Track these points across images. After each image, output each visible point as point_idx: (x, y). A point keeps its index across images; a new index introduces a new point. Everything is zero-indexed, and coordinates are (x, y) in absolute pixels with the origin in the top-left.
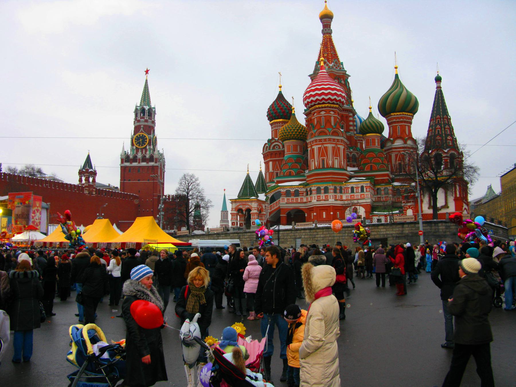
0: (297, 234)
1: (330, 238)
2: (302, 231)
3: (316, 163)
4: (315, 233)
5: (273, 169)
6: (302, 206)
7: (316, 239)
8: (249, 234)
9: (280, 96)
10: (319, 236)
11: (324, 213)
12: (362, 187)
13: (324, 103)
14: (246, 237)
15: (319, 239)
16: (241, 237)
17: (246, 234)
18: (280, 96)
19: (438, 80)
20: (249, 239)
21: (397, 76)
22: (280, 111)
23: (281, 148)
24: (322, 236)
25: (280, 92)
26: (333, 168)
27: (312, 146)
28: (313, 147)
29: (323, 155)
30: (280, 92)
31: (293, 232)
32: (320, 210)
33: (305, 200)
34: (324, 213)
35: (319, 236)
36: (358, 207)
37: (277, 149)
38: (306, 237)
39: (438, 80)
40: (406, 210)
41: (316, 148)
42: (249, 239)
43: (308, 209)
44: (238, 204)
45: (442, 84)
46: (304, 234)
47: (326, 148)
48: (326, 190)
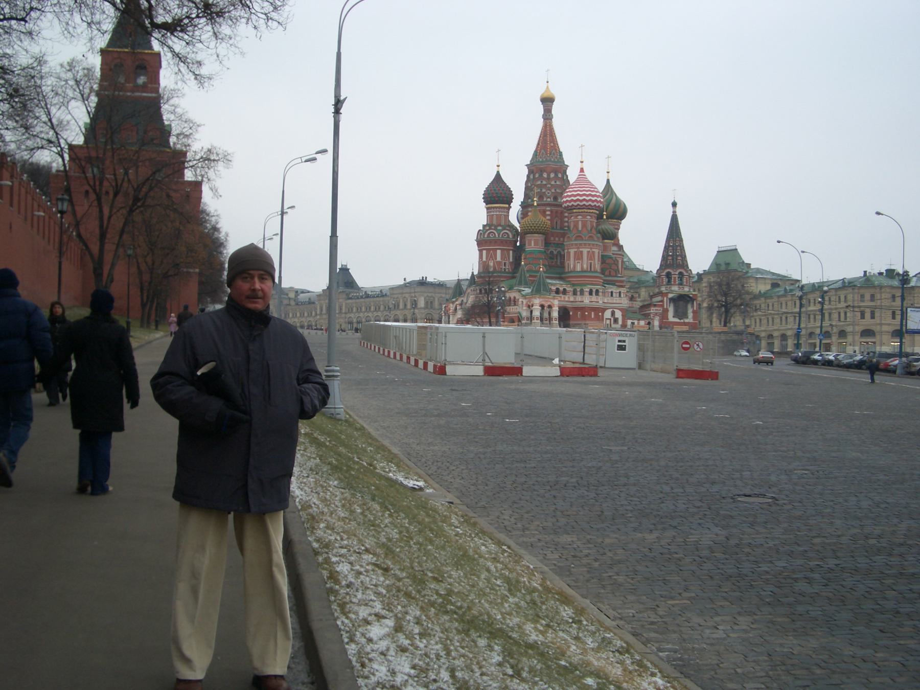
3: (585, 266)
6: (569, 305)
9: (498, 177)
12: (620, 293)
18: (498, 177)
19: (674, 205)
21: (608, 181)
22: (497, 195)
25: (498, 172)
26: (596, 272)
29: (591, 259)
30: (498, 172)
33: (572, 299)
39: (674, 205)
41: (585, 251)
45: (678, 209)
47: (593, 252)
48: (597, 292)
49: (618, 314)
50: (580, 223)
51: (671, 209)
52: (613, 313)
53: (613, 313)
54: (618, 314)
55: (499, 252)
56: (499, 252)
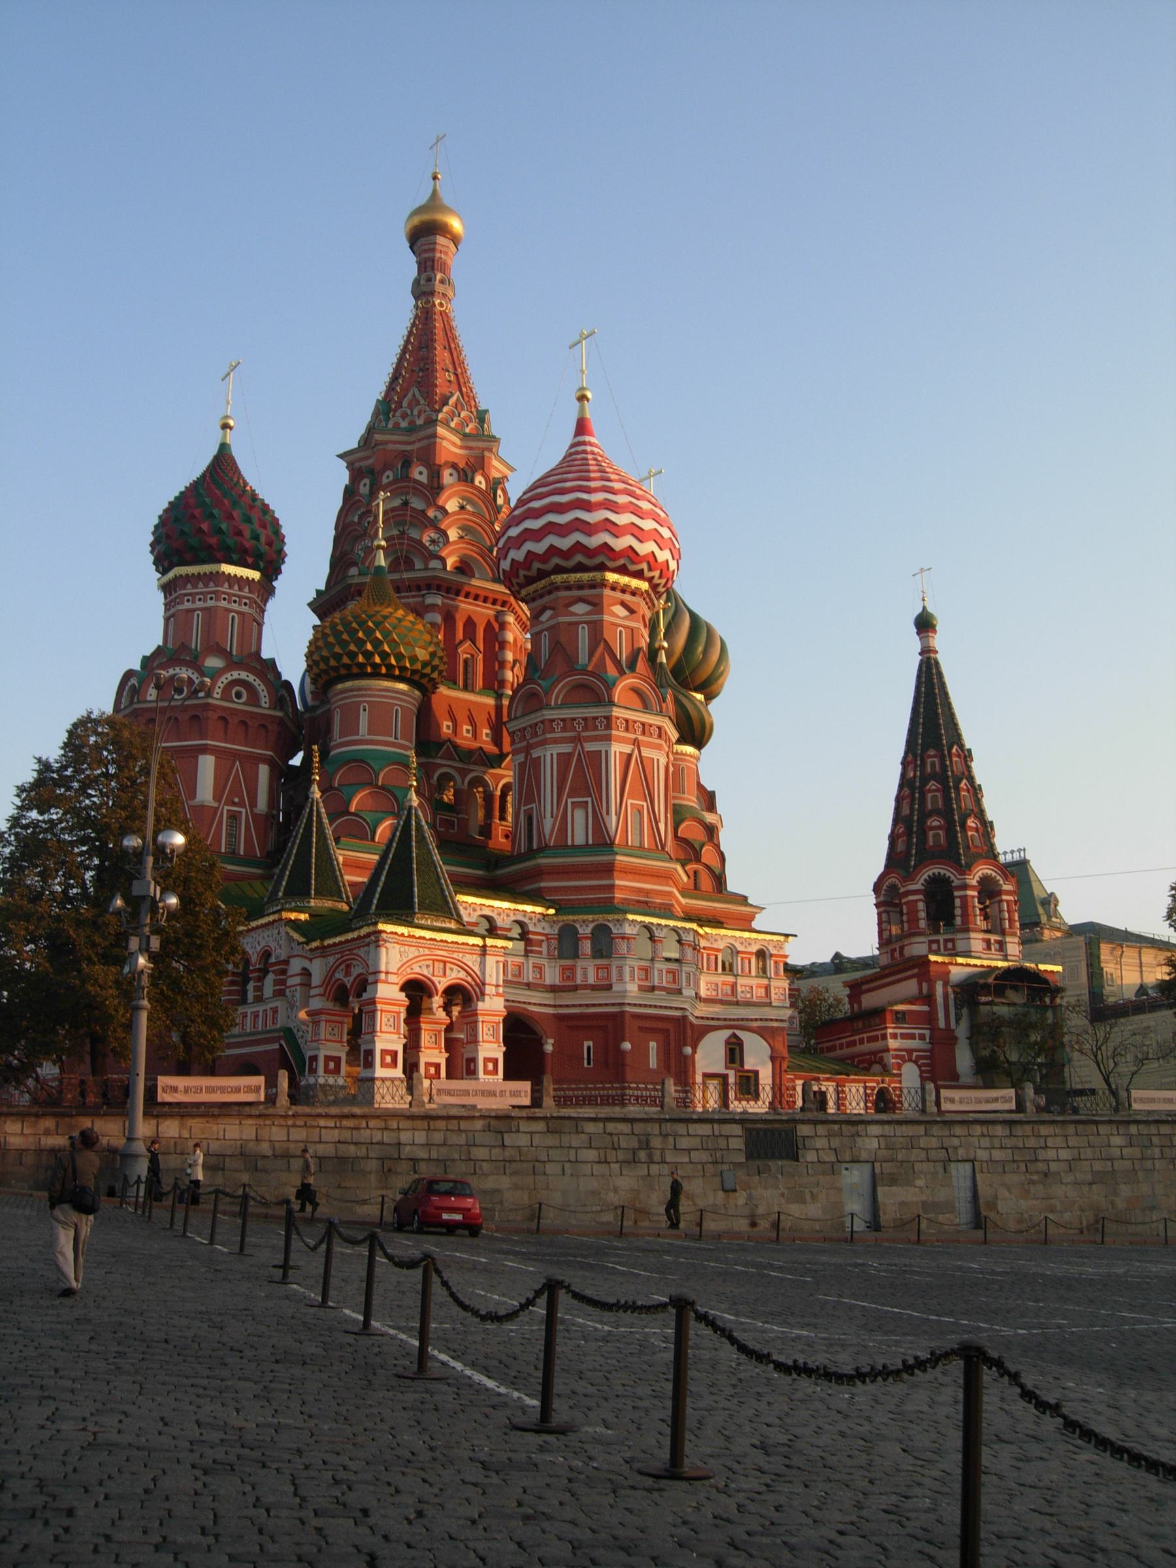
0: (956, 1142)
1: (1098, 1166)
2: (978, 1130)
4: (1032, 1142)
5: (217, 796)
7: (1041, 1166)
8: (705, 1129)
9: (223, 465)
10: (1051, 1154)
11: (653, 1045)
13: (639, 575)
14: (684, 1143)
15: (1054, 1167)
16: (656, 1142)
17: (681, 1128)
18: (223, 465)
19: (924, 624)
20: (704, 1157)
23: (265, 700)
24: (1064, 1154)
27: (578, 740)
28: (590, 747)
30: (224, 448)
31: (935, 1130)
32: (641, 1029)
34: (653, 1045)
35: (1051, 1154)
36: (739, 1033)
37: (239, 705)
38: (997, 1155)
39: (924, 624)
40: (899, 1067)
42: (704, 1157)
43: (560, 1018)
44: (412, 952)
46: (985, 1142)
49: (758, 1057)
50: (583, 634)
51: (916, 644)
52: (734, 1051)
53: (734, 1051)
54: (758, 1057)
55: (207, 765)
56: (207, 765)
